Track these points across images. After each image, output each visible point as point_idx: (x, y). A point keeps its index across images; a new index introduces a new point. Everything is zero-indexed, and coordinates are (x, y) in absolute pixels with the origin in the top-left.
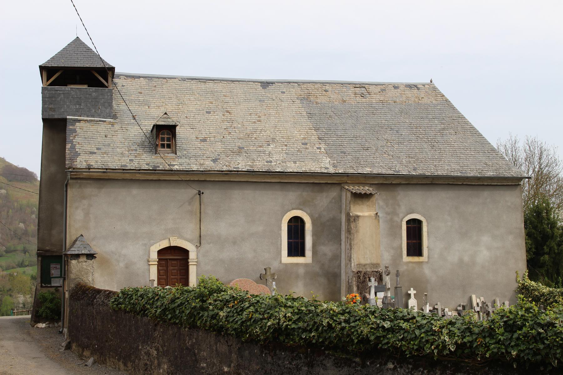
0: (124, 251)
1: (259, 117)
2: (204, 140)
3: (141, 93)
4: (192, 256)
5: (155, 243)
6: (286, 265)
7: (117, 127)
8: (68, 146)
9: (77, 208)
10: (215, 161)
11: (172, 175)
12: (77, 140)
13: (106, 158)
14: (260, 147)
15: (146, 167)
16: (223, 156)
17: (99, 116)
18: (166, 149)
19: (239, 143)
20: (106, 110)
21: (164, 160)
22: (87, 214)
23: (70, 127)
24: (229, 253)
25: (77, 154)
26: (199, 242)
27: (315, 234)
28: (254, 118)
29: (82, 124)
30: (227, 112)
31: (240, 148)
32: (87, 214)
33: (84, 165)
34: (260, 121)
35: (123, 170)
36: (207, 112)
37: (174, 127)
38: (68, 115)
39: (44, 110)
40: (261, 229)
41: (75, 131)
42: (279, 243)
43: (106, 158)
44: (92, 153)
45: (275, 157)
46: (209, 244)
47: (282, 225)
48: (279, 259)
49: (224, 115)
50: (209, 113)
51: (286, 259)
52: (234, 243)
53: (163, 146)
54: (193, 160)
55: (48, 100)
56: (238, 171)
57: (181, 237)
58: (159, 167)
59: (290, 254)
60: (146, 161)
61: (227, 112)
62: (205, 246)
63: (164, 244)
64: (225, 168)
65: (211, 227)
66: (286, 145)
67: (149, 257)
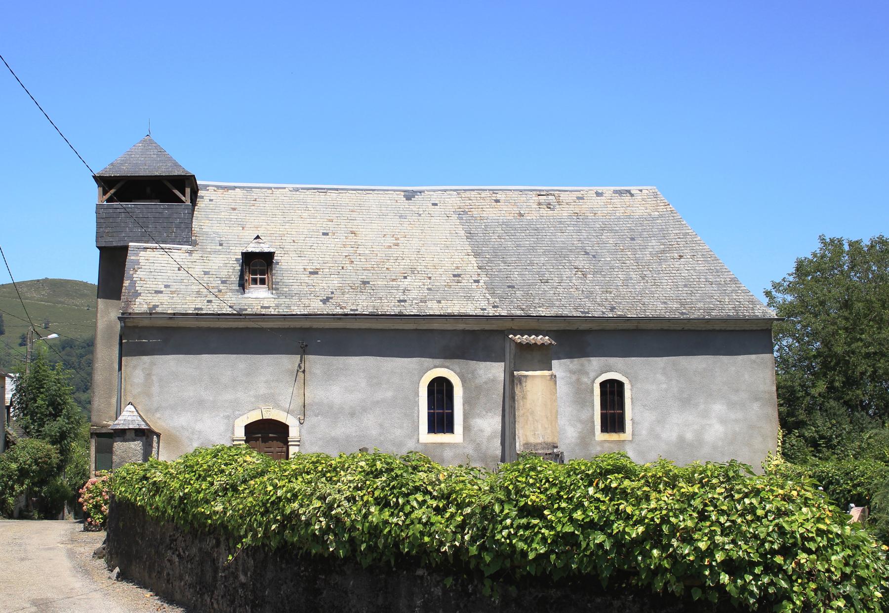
0: (199, 426)
1: (397, 239)
2: (315, 273)
3: (234, 209)
4: (293, 433)
5: (241, 415)
6: (426, 444)
7: (196, 256)
8: (126, 283)
9: (135, 367)
10: (325, 301)
11: (264, 320)
12: (139, 274)
13: (176, 299)
14: (393, 280)
15: (229, 311)
16: (338, 293)
17: (173, 242)
18: (259, 286)
19: (364, 276)
20: (182, 234)
21: (258, 298)
22: (148, 376)
23: (131, 257)
24: (344, 429)
25: (137, 294)
26: (303, 412)
27: (467, 402)
28: (390, 241)
29: (149, 253)
30: (352, 232)
31: (365, 283)
32: (148, 376)
33: (144, 308)
34: (397, 245)
35: (197, 314)
36: (324, 234)
37: (270, 255)
38: (132, 241)
39: (99, 236)
40: (389, 394)
41: (138, 263)
42: (416, 415)
43: (176, 299)
44: (157, 292)
45: (414, 294)
46: (316, 416)
47: (420, 389)
48: (416, 437)
49: (346, 238)
50: (326, 234)
51: (426, 437)
52: (352, 414)
53: (255, 281)
54: (295, 299)
55: (103, 220)
56: (356, 315)
57: (277, 406)
58: (246, 310)
59: (432, 429)
60: (228, 301)
61: (352, 232)
62: (311, 421)
63: (255, 416)
64: (338, 311)
65: (317, 393)
66: (430, 278)
67: (233, 433)
